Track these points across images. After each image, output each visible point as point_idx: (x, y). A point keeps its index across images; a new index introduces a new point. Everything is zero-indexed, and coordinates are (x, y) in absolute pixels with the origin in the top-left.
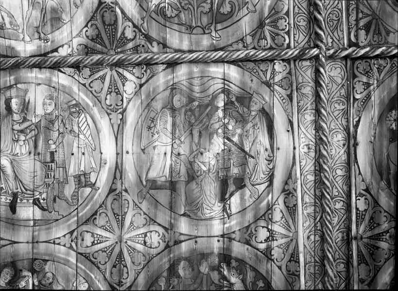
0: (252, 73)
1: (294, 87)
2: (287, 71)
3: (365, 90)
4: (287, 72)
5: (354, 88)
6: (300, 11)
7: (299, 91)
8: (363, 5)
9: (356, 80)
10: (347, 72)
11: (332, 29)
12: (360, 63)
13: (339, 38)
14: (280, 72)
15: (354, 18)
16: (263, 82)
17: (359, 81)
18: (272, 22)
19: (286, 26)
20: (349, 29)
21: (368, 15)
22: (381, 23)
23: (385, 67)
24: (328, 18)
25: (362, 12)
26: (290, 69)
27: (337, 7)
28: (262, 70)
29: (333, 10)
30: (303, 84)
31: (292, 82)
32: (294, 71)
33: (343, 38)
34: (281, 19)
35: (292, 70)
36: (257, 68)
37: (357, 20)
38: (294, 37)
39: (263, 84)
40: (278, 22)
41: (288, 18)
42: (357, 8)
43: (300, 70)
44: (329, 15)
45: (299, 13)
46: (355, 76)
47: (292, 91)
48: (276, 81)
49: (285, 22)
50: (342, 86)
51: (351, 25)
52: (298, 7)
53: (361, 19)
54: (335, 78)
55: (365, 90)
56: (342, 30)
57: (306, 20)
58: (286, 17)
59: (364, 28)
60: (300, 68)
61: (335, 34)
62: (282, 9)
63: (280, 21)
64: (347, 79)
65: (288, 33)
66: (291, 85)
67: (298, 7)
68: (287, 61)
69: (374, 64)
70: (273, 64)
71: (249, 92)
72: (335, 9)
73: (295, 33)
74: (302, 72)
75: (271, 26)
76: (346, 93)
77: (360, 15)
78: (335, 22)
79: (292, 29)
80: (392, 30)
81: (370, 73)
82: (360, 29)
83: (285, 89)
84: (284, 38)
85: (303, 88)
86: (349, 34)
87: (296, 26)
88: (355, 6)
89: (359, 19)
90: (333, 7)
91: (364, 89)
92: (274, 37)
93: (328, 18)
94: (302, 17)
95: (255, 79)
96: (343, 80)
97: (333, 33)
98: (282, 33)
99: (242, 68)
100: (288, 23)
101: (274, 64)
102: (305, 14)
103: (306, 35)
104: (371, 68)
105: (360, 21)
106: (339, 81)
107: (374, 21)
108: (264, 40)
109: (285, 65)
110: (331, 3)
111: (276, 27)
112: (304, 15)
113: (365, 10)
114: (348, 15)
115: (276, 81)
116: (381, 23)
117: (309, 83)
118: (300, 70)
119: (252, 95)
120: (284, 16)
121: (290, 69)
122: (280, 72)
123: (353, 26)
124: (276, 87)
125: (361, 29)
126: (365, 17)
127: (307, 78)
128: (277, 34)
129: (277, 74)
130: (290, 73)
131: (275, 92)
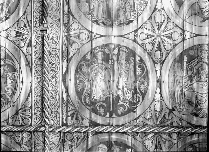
0: (11, 137)
1: (33, 146)
2: (30, 137)
3: (70, 148)
4: (30, 138)
5: (64, 147)
6: (38, 106)
7: (36, 148)
8: (70, 104)
9: (65, 143)
10: (61, 139)
11: (53, 116)
12: (68, 134)
13: (58, 121)
14: (26, 138)
15: (65, 111)
16: (17, 143)
17: (67, 144)
18: (23, 112)
19: (30, 114)
20: (63, 116)
21: (73, 110)
22: (80, 114)
23: (80, 137)
24: (52, 111)
25: (70, 108)
26: (32, 136)
27: (57, 105)
28: (17, 136)
29: (54, 106)
30: (38, 144)
31: (32, 143)
32: (33, 137)
33: (60, 121)
34: (28, 110)
35: (32, 137)
36: (14, 135)
37: (67, 112)
38: (34, 120)
39: (17, 144)
40: (26, 111)
41: (31, 109)
42: (67, 106)
43: (37, 137)
44: (52, 109)
45: (37, 107)
46: (65, 141)
47: (32, 147)
48: (24, 142)
49: (30, 112)
50: (58, 146)
51: (64, 115)
52: (37, 104)
53: (69, 111)
54: (55, 142)
55: (70, 148)
56: (59, 117)
57: (40, 111)
58: (30, 109)
59: (70, 116)
60: (37, 136)
61: (55, 119)
62: (28, 105)
63: (27, 111)
64: (61, 142)
65: (31, 117)
66: (32, 144)
67: (37, 104)
68: (31, 132)
69: (75, 135)
70: (22, 133)
71: (9, 147)
72: (56, 106)
73: (35, 118)
74: (37, 138)
75: (22, 114)
76: (60, 150)
77: (69, 110)
78: (56, 113)
79: (33, 115)
80: (85, 118)
81: (73, 140)
82: (68, 116)
83: (28, 147)
84: (29, 120)
85: (38, 146)
86: (63, 119)
87: (35, 114)
88: (66, 105)
89: (68, 111)
90: (54, 105)
91: (69, 148)
92: (24, 119)
93: (52, 111)
94: (38, 110)
95: (13, 141)
96: (58, 143)
97: (54, 119)
98: (27, 117)
99: (7, 135)
100: (31, 112)
101: (23, 133)
102: (40, 108)
103: (40, 119)
104: (73, 137)
105: (68, 113)
106: (57, 143)
107: (76, 113)
108: (18, 121)
109: (29, 134)
110: (54, 103)
111: (25, 114)
112: (40, 109)
113: (71, 107)
114: (62, 109)
115: (24, 142)
116: (80, 114)
117: (41, 144)
118: (37, 137)
119: (11, 149)
120: (29, 108)
121: (32, 136)
122: (26, 138)
123: (64, 115)
124: (24, 146)
125: (69, 117)
126: (71, 111)
127: (40, 141)
128: (25, 118)
129: (24, 139)
130: (31, 138)
131: (23, 148)
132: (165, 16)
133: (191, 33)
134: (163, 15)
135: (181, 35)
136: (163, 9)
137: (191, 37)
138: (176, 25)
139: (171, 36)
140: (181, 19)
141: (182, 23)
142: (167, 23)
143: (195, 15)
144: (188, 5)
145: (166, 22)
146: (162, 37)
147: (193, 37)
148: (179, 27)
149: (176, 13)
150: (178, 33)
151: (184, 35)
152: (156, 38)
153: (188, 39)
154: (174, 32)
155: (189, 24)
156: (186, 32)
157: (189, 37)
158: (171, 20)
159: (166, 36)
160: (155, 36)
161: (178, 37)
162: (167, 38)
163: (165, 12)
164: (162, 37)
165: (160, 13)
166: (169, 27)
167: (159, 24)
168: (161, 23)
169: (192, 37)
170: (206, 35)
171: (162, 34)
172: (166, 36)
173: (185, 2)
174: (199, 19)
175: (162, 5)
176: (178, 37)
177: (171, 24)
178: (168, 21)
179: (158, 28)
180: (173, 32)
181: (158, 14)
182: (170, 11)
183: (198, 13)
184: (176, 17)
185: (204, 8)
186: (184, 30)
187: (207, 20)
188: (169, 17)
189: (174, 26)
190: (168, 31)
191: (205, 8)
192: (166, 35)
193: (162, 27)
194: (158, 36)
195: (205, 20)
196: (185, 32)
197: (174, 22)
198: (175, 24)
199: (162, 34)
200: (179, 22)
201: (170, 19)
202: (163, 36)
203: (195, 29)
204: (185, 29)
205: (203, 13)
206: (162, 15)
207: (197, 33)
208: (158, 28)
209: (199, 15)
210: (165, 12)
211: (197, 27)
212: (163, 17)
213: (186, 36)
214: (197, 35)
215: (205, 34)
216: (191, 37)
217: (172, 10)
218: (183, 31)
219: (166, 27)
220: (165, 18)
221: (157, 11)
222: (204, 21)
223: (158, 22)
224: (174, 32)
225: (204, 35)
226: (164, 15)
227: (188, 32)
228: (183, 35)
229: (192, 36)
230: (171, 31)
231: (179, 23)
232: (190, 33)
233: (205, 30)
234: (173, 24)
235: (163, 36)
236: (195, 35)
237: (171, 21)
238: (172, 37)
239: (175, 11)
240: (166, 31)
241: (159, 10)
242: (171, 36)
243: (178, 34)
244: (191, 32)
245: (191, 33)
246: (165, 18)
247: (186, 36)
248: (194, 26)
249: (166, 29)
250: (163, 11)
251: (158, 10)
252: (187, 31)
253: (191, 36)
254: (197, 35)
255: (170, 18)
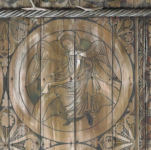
132: (14, 118)
133: (51, 140)
134: (12, 116)
135: (37, 143)
136: (12, 108)
137: (51, 146)
138: (30, 129)
139: (24, 145)
140: (36, 121)
141: (38, 126)
142: (18, 128)
143: (56, 115)
144: (46, 101)
145: (15, 126)
146: (11, 147)
147: (54, 146)
148: (34, 132)
149: (30, 114)
150: (32, 141)
151: (42, 144)
152: (2, 148)
153: (47, 148)
154: (27, 139)
155: (48, 127)
156: (44, 140)
157: (48, 146)
158: (22, 123)
159: (17, 145)
160: (1, 146)
161: (33, 146)
162: (18, 148)
163: (15, 113)
164: (11, 147)
165: (8, 113)
166: (20, 133)
167: (6, 129)
168: (10, 128)
169: (52, 146)
170: (71, 143)
171: (11, 143)
172: (17, 145)
173: (41, 97)
174: (61, 120)
175: (10, 102)
176: (33, 146)
177: (23, 129)
178: (19, 124)
179: (5, 135)
180: (26, 140)
181: (5, 115)
182: (20, 110)
183: (60, 112)
184: (29, 119)
185: (68, 106)
186: (41, 136)
187: (71, 123)
188: (20, 120)
189: (27, 131)
190: (19, 138)
191: (70, 105)
192: (16, 143)
193: (10, 133)
194: (5, 145)
195: (70, 122)
196: (43, 139)
197: (27, 126)
198: (28, 129)
199: (11, 143)
200: (33, 125)
201: (21, 121)
202: (12, 145)
203: (56, 135)
204: (42, 135)
205: (67, 112)
206: (10, 117)
207: (59, 140)
208: (5, 134)
209: (61, 116)
210: (15, 113)
211: (58, 133)
212: (11, 119)
213: (45, 145)
214: (59, 144)
215: (69, 142)
216: (51, 146)
217: (24, 109)
218: (40, 137)
219: (15, 133)
220: (14, 120)
221: (3, 111)
222: (68, 123)
223: (4, 126)
224: (27, 139)
225: (68, 144)
226: (12, 117)
227: (47, 139)
228: (40, 144)
229: (51, 145)
230: (24, 138)
231: (34, 127)
232: (50, 141)
233: (70, 136)
234: (26, 129)
235: (12, 145)
236: (55, 143)
237: (23, 124)
238: (25, 147)
239: (28, 111)
240: (17, 138)
241: (5, 110)
242: (23, 145)
243: (33, 142)
244: (50, 140)
245: (51, 140)
246: (14, 120)
247: (43, 144)
248: (54, 130)
249: (16, 135)
250: (11, 111)
251: (4, 110)
252: (46, 138)
253: (50, 144)
254: (59, 144)
255: (22, 120)
